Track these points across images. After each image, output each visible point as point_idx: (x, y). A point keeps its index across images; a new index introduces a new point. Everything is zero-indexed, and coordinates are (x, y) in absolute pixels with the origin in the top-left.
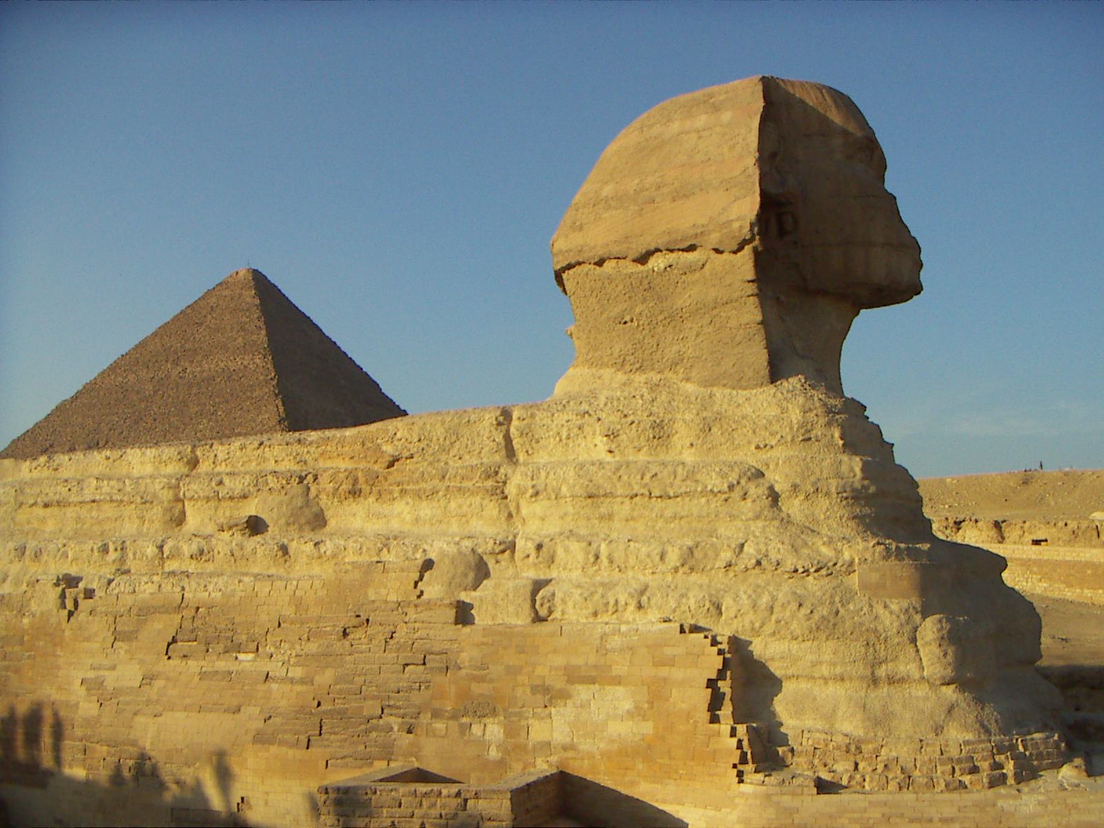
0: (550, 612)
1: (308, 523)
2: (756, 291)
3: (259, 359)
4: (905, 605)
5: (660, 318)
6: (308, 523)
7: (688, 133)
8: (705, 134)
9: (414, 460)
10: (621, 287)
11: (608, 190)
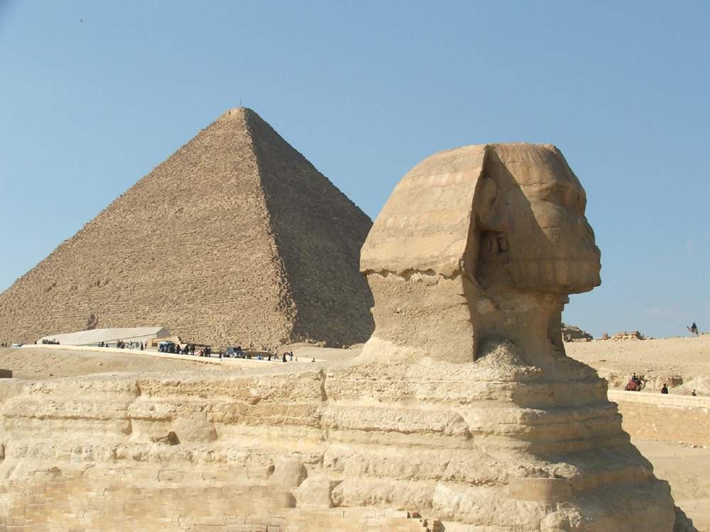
0: (340, 501)
1: (206, 437)
2: (466, 301)
3: (253, 197)
4: (536, 505)
5: (417, 311)
6: (206, 437)
7: (437, 186)
8: (447, 188)
9: (269, 400)
10: (395, 289)
11: (390, 222)
